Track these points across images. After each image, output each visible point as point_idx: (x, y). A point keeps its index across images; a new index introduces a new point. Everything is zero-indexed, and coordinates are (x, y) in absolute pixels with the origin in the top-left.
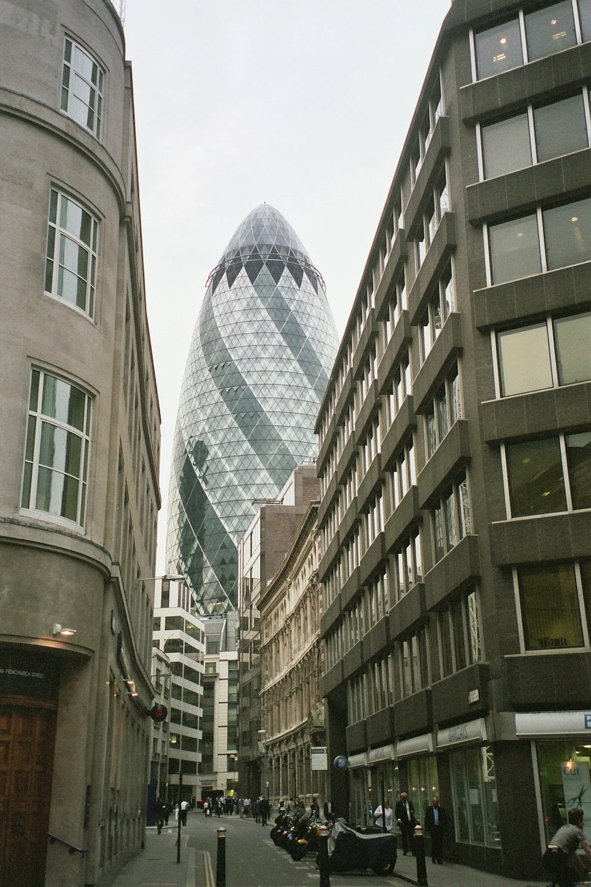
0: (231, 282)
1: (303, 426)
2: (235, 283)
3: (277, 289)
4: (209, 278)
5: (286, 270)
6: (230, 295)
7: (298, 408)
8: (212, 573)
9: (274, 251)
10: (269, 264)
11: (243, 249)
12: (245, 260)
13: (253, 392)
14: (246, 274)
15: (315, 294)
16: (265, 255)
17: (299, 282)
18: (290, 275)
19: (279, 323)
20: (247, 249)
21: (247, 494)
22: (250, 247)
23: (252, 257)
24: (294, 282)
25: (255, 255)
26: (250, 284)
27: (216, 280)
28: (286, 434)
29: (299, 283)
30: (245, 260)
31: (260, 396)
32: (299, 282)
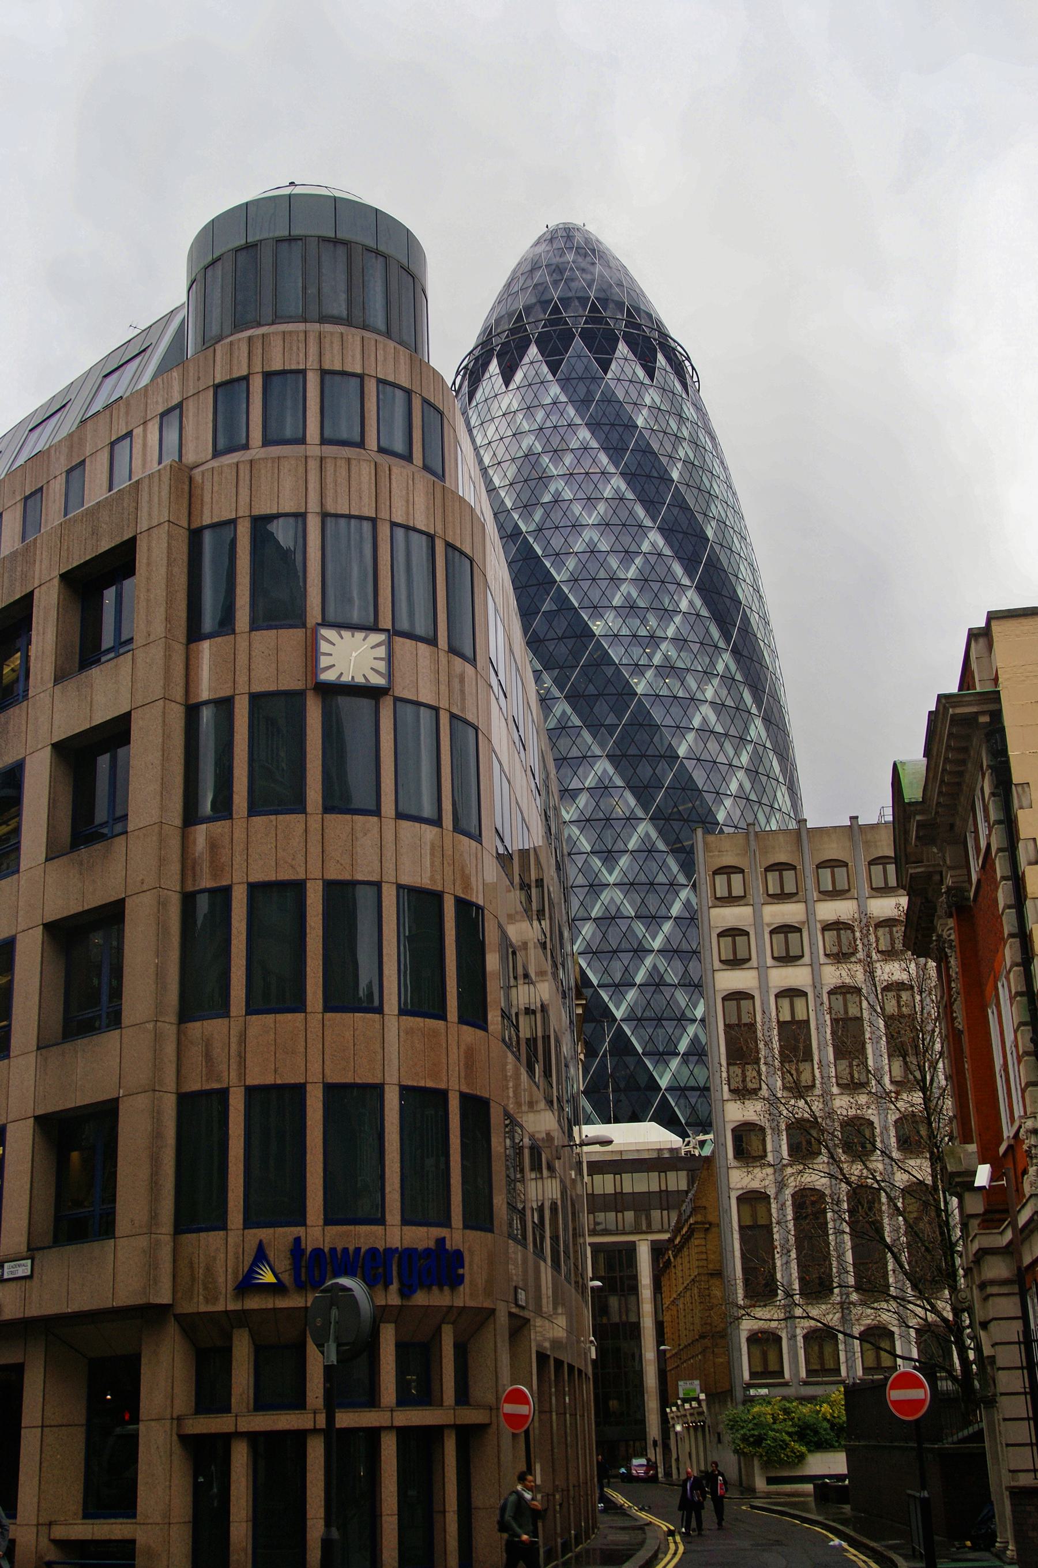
0: (507, 377)
1: (680, 664)
2: (519, 376)
5: (622, 348)
6: (510, 400)
9: (594, 308)
10: (585, 335)
12: (534, 330)
16: (576, 318)
18: (631, 356)
19: (615, 452)
20: (538, 308)
23: (550, 323)
25: (556, 319)
26: (550, 377)
28: (644, 682)
29: (650, 373)
30: (534, 330)
31: (586, 603)
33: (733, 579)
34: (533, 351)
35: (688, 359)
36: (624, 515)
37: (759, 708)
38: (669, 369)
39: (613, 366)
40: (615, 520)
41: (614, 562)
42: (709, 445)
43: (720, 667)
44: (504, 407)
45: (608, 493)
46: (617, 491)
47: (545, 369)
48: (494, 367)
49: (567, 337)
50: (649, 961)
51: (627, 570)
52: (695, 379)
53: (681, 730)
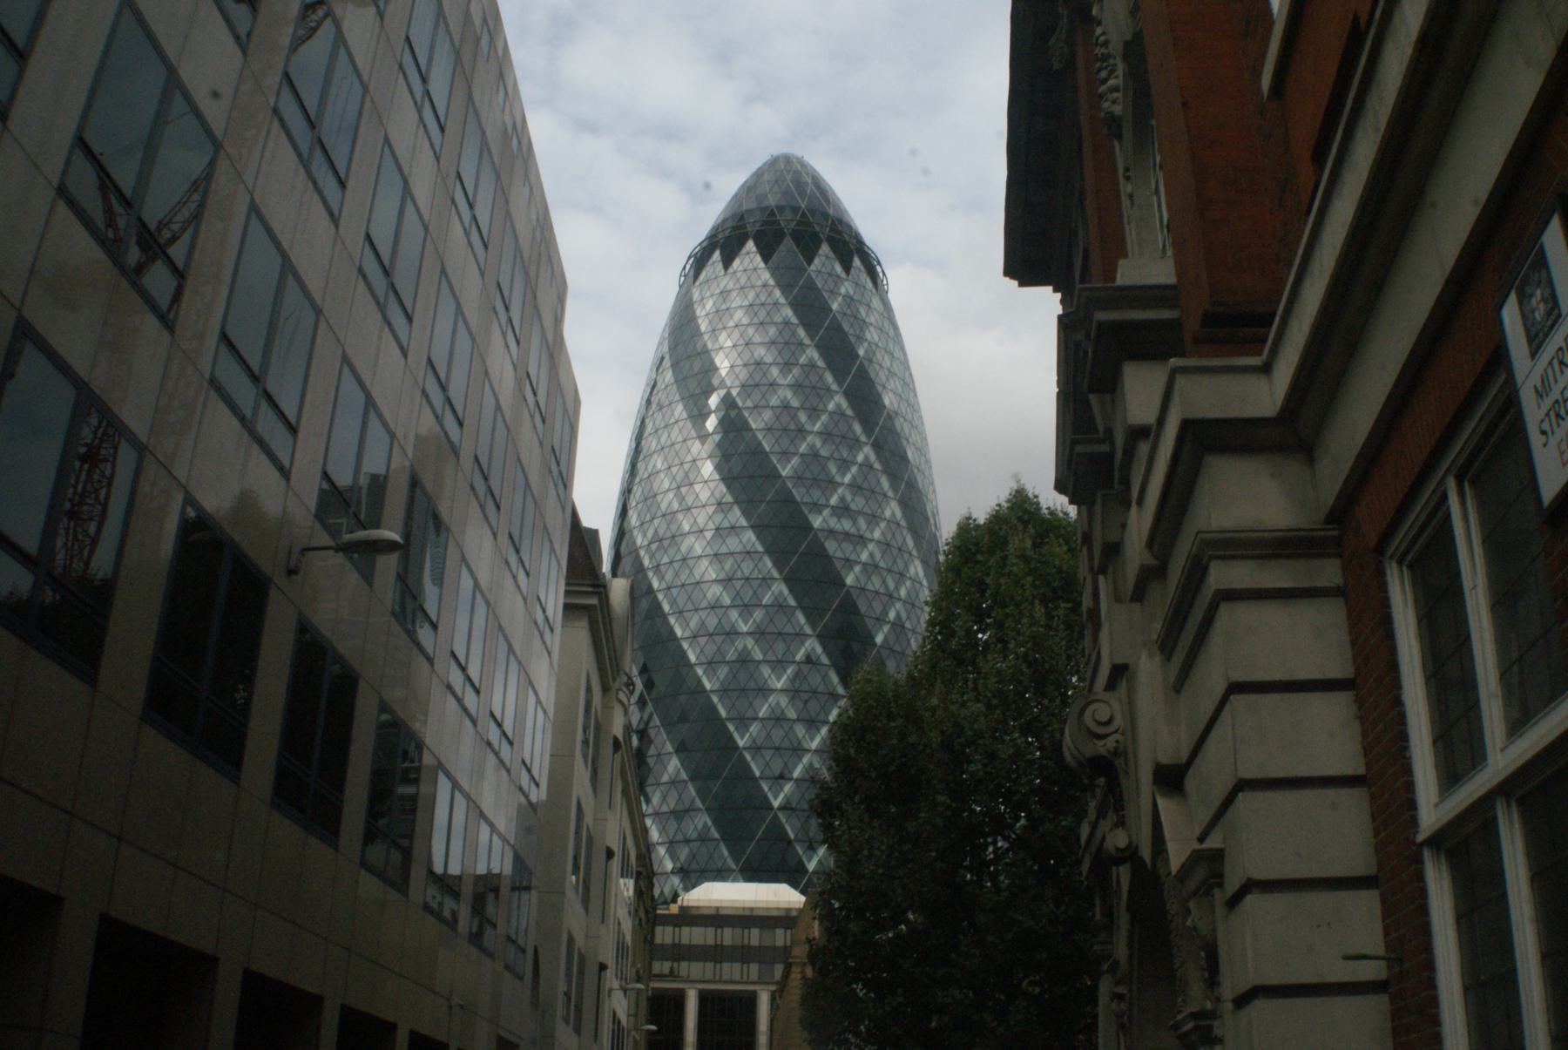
0: (727, 262)
1: (853, 507)
2: (736, 263)
3: (809, 274)
4: (689, 258)
6: (726, 282)
7: (844, 475)
8: (676, 766)
11: (750, 212)
13: (764, 443)
14: (754, 249)
15: (874, 291)
16: (787, 221)
17: (847, 267)
18: (832, 255)
19: (811, 328)
21: (746, 622)
22: (763, 210)
23: (765, 223)
24: (838, 269)
26: (762, 265)
27: (700, 261)
32: (847, 267)
33: (905, 442)
34: (750, 245)
35: (879, 263)
36: (814, 379)
37: (919, 551)
38: (862, 268)
39: (816, 261)
40: (807, 383)
41: (803, 417)
42: (892, 333)
43: (888, 513)
44: (722, 286)
45: (803, 360)
46: (811, 360)
47: (758, 258)
48: (717, 255)
49: (779, 236)
50: (806, 759)
51: (814, 425)
52: (885, 282)
53: (849, 563)
